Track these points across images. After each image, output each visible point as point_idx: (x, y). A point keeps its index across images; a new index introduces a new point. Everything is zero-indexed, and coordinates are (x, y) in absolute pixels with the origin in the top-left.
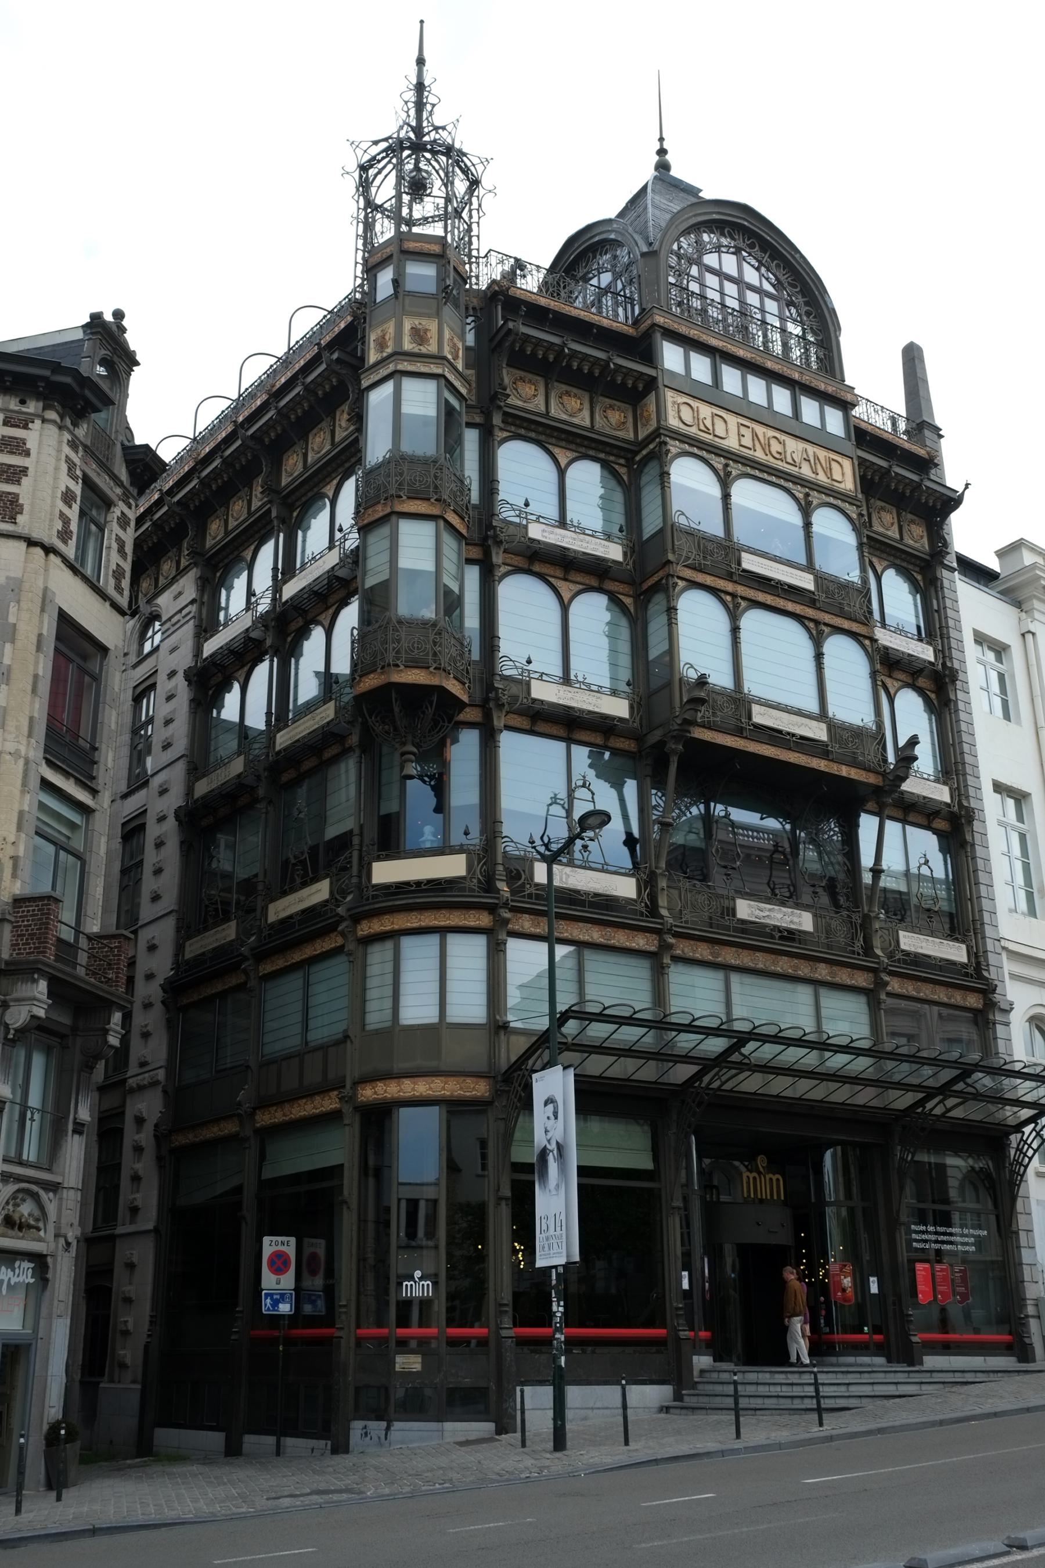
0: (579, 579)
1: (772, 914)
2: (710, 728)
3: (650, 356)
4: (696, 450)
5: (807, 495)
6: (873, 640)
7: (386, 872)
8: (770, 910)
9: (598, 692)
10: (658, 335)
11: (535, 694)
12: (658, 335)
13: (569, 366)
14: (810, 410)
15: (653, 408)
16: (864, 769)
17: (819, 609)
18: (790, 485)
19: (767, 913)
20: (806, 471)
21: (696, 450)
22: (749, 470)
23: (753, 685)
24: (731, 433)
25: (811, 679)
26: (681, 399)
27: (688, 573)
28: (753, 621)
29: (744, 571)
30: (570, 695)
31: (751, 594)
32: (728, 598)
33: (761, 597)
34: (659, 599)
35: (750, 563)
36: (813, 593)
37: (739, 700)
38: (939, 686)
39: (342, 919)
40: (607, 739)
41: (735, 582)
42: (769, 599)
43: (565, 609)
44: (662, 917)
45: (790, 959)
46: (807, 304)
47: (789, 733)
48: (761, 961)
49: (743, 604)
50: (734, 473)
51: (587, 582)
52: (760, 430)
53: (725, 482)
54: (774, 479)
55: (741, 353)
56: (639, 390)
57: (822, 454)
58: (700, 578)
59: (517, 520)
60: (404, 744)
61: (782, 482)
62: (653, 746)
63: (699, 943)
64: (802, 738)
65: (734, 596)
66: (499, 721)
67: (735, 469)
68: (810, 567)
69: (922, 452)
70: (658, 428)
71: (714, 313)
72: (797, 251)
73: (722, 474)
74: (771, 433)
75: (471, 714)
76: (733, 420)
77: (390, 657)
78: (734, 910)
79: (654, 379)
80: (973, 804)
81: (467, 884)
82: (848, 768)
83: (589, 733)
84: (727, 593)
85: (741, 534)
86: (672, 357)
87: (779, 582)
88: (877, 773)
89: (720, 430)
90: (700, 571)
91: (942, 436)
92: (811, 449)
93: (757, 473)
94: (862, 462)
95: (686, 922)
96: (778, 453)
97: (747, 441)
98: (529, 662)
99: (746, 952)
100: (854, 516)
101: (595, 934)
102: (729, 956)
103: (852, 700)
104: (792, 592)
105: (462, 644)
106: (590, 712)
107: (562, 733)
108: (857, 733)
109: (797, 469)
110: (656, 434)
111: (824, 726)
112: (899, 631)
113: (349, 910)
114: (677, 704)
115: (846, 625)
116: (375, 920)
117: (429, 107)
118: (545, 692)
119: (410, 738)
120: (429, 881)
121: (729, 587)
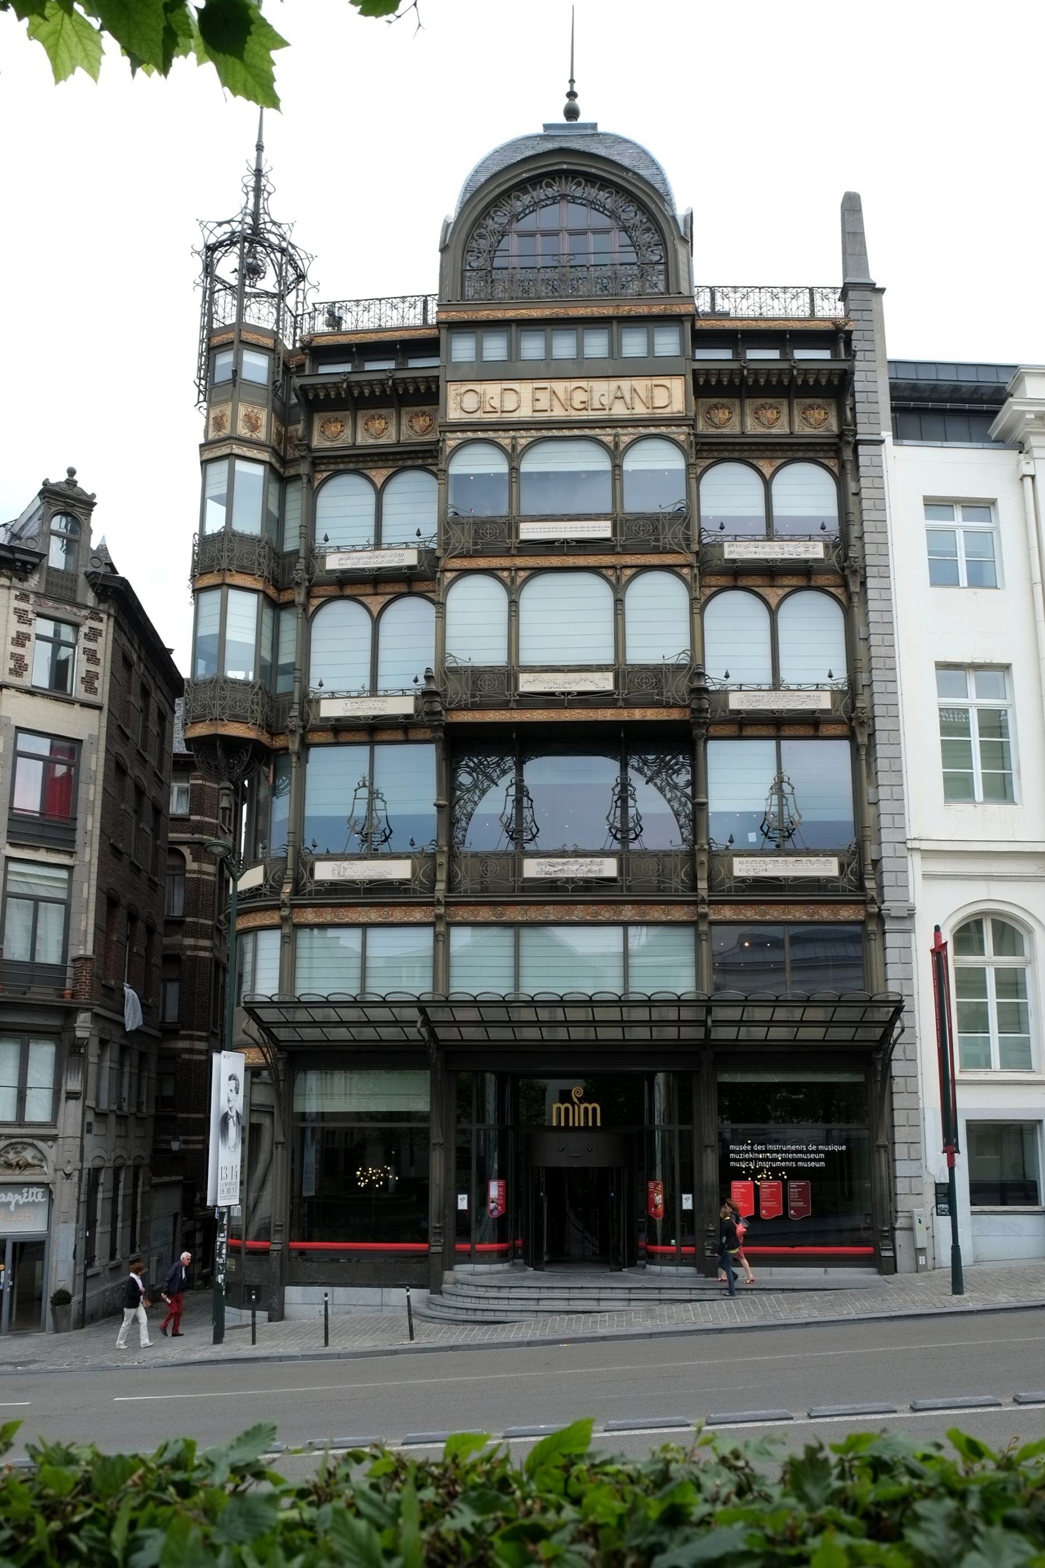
0: (388, 590)
1: (566, 868)
4: (481, 435)
5: (616, 435)
8: (563, 864)
16: (664, 707)
17: (618, 553)
19: (560, 867)
22: (545, 433)
26: (464, 389)
32: (505, 574)
40: (406, 733)
45: (586, 907)
47: (563, 693)
48: (551, 913)
52: (559, 386)
54: (576, 432)
63: (479, 908)
64: (580, 693)
73: (509, 448)
76: (525, 389)
81: (264, 891)
82: (642, 711)
83: (389, 732)
84: (503, 569)
87: (565, 541)
89: (510, 403)
93: (555, 433)
95: (466, 891)
96: (582, 402)
97: (544, 404)
99: (533, 908)
102: (514, 914)
106: (375, 717)
109: (606, 412)
117: (266, 195)
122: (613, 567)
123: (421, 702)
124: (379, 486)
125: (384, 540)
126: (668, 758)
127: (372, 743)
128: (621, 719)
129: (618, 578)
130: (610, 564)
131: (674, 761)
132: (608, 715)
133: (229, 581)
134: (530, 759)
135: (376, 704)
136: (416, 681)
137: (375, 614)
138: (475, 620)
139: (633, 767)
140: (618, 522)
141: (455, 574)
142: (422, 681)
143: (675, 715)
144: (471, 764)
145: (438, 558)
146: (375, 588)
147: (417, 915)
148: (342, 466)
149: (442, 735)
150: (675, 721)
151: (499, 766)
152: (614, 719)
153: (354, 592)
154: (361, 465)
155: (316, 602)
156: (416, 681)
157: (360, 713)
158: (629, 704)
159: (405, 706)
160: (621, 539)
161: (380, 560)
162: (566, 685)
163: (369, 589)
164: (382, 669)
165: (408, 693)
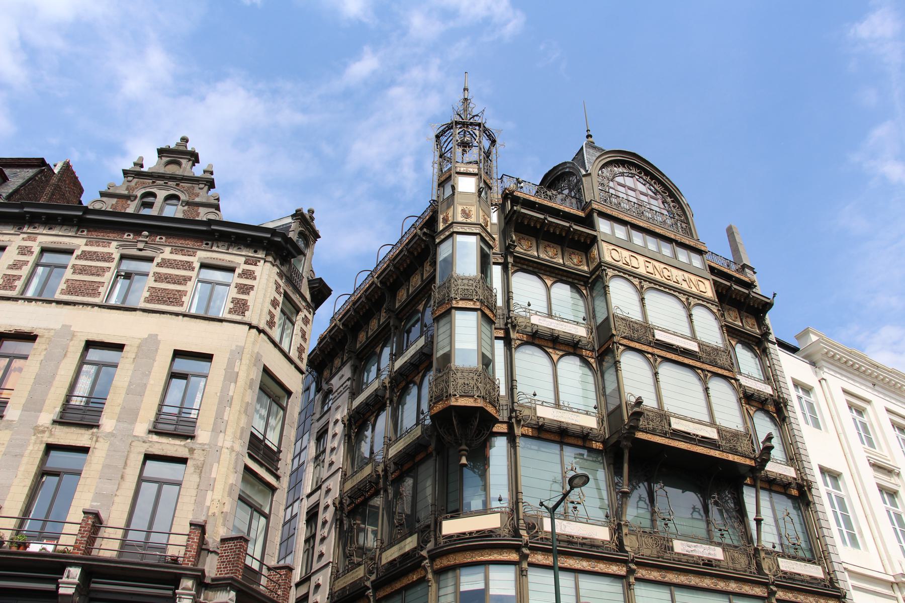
2: (647, 433)
3: (591, 225)
4: (621, 274)
5: (687, 299)
6: (737, 380)
7: (450, 527)
10: (595, 215)
11: (539, 414)
12: (595, 215)
13: (548, 231)
14: (683, 256)
15: (596, 252)
17: (703, 362)
18: (676, 294)
20: (685, 286)
21: (621, 274)
22: (652, 285)
23: (670, 406)
24: (641, 266)
25: (703, 403)
27: (625, 342)
28: (666, 371)
31: (663, 353)
34: (608, 359)
35: (660, 336)
37: (664, 416)
38: (776, 408)
39: (424, 558)
43: (554, 365)
44: (627, 552)
46: (673, 202)
48: (694, 581)
49: (659, 360)
50: (645, 287)
53: (640, 292)
54: (667, 290)
55: (641, 224)
56: (586, 244)
57: (693, 278)
58: (633, 344)
59: (523, 314)
60: (461, 445)
61: (672, 292)
62: (613, 445)
64: (703, 437)
65: (652, 354)
66: (518, 431)
67: (646, 285)
68: (694, 338)
69: (747, 279)
70: (601, 262)
71: (625, 205)
72: (664, 175)
74: (663, 266)
75: (501, 428)
77: (451, 391)
78: (672, 548)
79: (595, 237)
80: (810, 478)
84: (649, 353)
85: (653, 320)
86: (603, 226)
87: (678, 347)
88: (751, 458)
91: (755, 273)
92: (686, 275)
93: (657, 287)
94: (715, 282)
98: (535, 395)
100: (715, 311)
101: (585, 565)
102: (671, 577)
103: (730, 414)
104: (686, 352)
105: (494, 383)
107: (557, 438)
108: (736, 435)
110: (599, 265)
111: (715, 430)
112: (748, 376)
113: (428, 552)
114: (626, 417)
115: (720, 371)
116: (444, 558)
118: (546, 413)
119: (464, 441)
120: (478, 532)
121: (650, 350)
127: (562, 443)
129: (706, 376)
132: (716, 454)
133: (483, 308)
138: (634, 376)
143: (748, 462)
147: (614, 569)
148: (525, 267)
149: (629, 444)
154: (536, 270)
155: (518, 342)
163: (550, 344)
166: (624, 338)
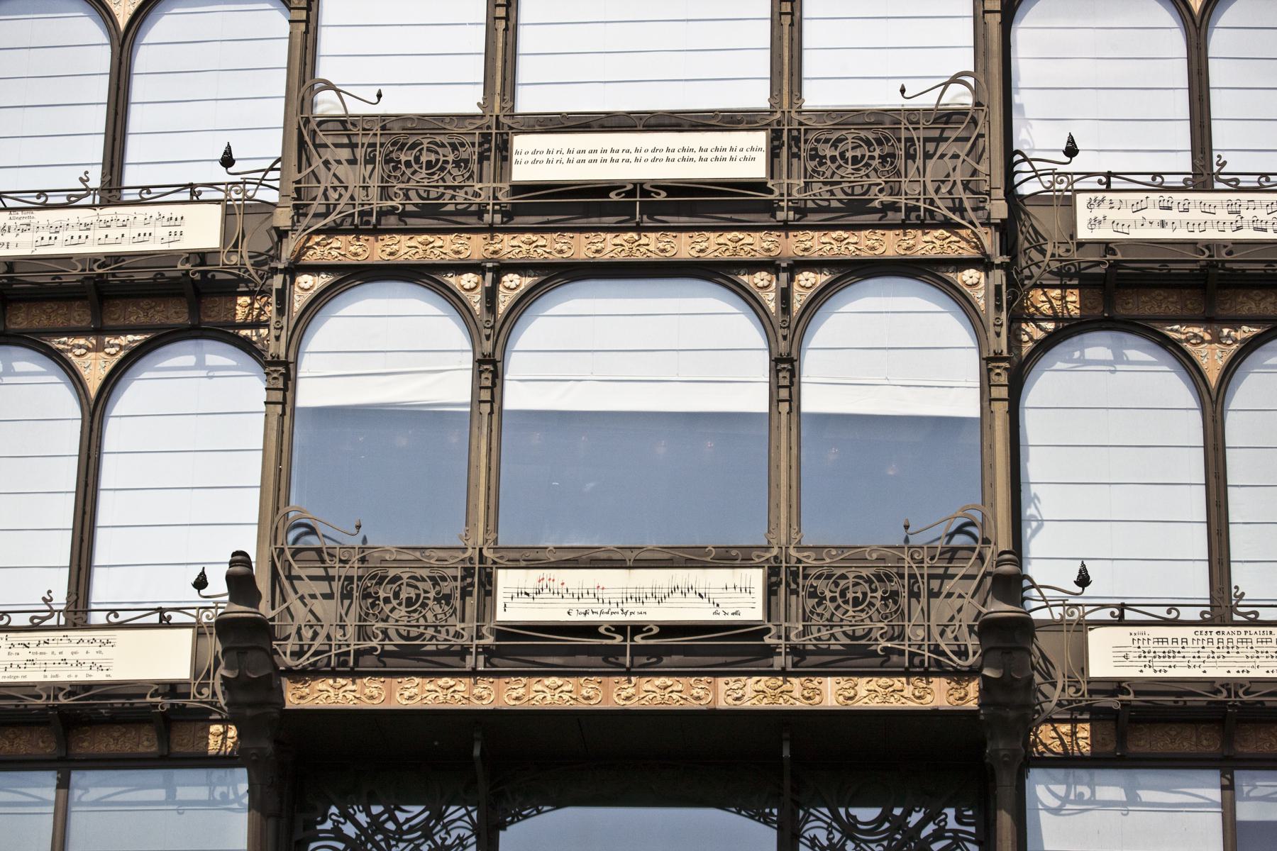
2: (354, 674)
9: (110, 626)
16: (907, 673)
17: (786, 227)
29: (519, 189)
30: (25, 654)
32: (469, 279)
33: (581, 247)
36: (758, 186)
41: (492, 229)
42: (611, 246)
43: (95, 411)
47: (620, 629)
51: (158, 319)
64: (668, 630)
87: (639, 188)
90: (376, 231)
115: (889, 245)
121: (474, 247)
122: (770, 265)
123: (213, 645)
124: (123, 22)
125: (132, 176)
126: (915, 818)
127: (64, 765)
128: (783, 704)
130: (760, 256)
131: (930, 829)
134: (519, 817)
135: (81, 649)
136: (201, 583)
137: (93, 386)
139: (813, 840)
140: (787, 131)
141: (323, 280)
142: (218, 585)
143: (939, 695)
144: (349, 830)
145: (282, 234)
146: (98, 313)
150: (935, 713)
151: (428, 835)
152: (763, 705)
153: (36, 324)
156: (201, 583)
157: (33, 676)
158: (808, 662)
159: (165, 658)
160: (791, 186)
161: (114, 233)
162: (631, 606)
163: (81, 317)
164: (105, 547)
165: (177, 618)
166: (331, 231)
